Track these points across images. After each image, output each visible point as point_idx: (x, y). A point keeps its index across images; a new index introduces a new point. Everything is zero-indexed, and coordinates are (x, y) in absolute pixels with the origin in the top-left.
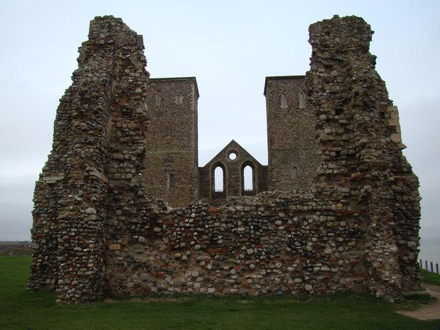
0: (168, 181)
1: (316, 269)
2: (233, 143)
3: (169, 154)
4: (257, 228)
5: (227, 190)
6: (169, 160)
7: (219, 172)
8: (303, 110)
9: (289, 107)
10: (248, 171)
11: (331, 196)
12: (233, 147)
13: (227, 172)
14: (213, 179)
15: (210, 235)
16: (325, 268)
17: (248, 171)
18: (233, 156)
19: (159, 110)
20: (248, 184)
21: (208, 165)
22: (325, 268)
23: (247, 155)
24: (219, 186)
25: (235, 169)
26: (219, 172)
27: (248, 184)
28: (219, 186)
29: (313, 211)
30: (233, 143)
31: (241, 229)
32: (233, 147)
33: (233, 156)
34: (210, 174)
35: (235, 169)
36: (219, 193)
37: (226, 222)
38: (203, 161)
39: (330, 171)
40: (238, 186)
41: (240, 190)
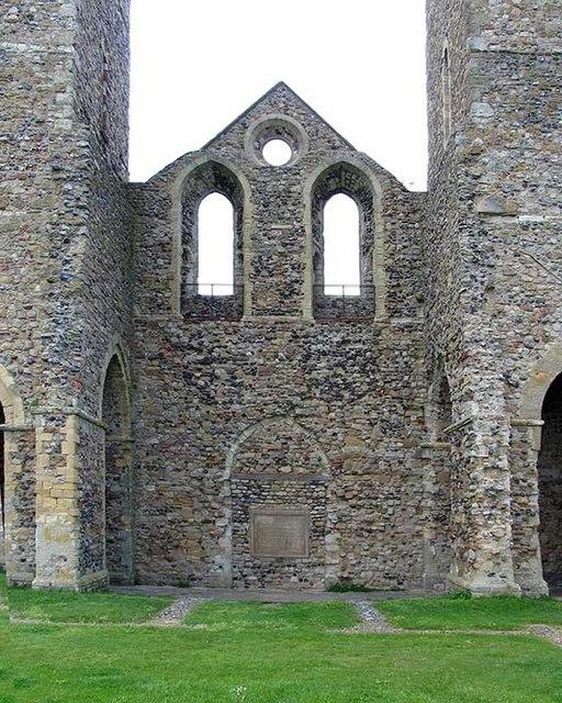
2: (280, 94)
5: (249, 288)
7: (215, 213)
10: (341, 214)
12: (280, 112)
13: (249, 207)
14: (189, 237)
17: (341, 214)
18: (277, 153)
20: (343, 273)
21: (168, 172)
23: (338, 142)
24: (215, 273)
25: (286, 196)
26: (215, 213)
27: (343, 273)
28: (215, 273)
30: (280, 94)
32: (280, 112)
33: (277, 153)
34: (177, 209)
35: (286, 196)
36: (212, 301)
38: (141, 167)
40: (298, 267)
41: (307, 288)
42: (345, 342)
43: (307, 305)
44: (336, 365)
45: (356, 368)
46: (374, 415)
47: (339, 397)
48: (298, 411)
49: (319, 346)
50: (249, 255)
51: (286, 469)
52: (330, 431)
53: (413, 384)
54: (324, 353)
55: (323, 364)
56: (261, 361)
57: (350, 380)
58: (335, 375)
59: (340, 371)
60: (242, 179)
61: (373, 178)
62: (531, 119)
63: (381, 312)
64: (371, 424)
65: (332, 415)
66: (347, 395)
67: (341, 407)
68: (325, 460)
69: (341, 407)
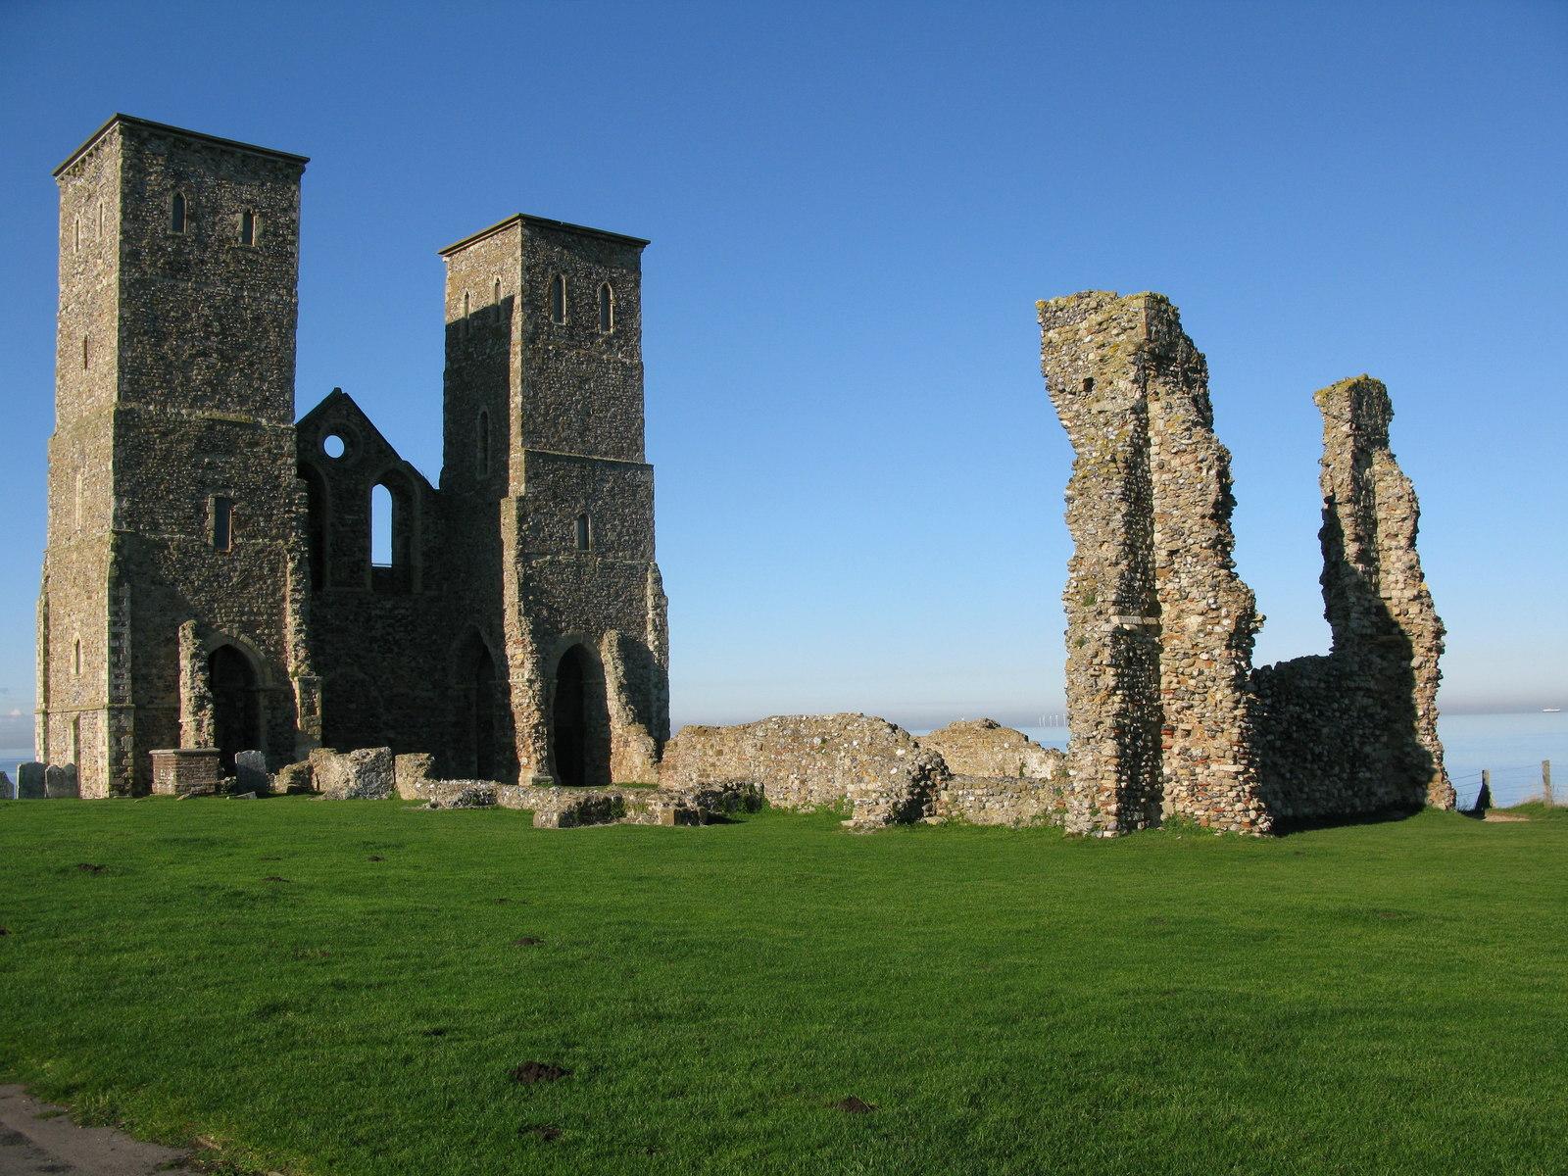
0: (211, 521)
1: (1361, 775)
3: (212, 424)
4: (1321, 713)
6: (215, 440)
8: (608, 342)
9: (570, 328)
10: (381, 500)
11: (1369, 667)
12: (339, 411)
15: (1285, 724)
16: (1368, 775)
17: (381, 500)
18: (334, 447)
19: (178, 252)
20: (382, 553)
22: (1368, 775)
23: (386, 451)
27: (382, 553)
29: (1359, 689)
31: (1309, 716)
32: (339, 411)
33: (334, 447)
37: (1297, 704)
39: (1364, 631)
42: (395, 608)
43: (368, 580)
44: (388, 625)
45: (402, 629)
46: (413, 664)
47: (391, 651)
48: (363, 661)
49: (378, 612)
50: (329, 539)
51: (353, 706)
52: (384, 677)
53: (439, 641)
54: (380, 617)
55: (379, 625)
56: (337, 623)
57: (397, 637)
58: (389, 634)
59: (390, 630)
60: (325, 478)
61: (415, 483)
62: (555, 496)
63: (417, 587)
64: (412, 671)
65: (385, 663)
66: (396, 650)
67: (392, 658)
68: (380, 699)
69: (392, 658)
